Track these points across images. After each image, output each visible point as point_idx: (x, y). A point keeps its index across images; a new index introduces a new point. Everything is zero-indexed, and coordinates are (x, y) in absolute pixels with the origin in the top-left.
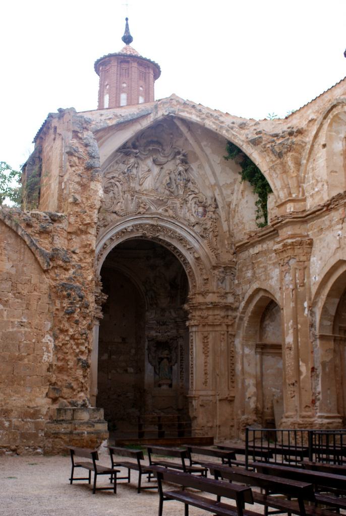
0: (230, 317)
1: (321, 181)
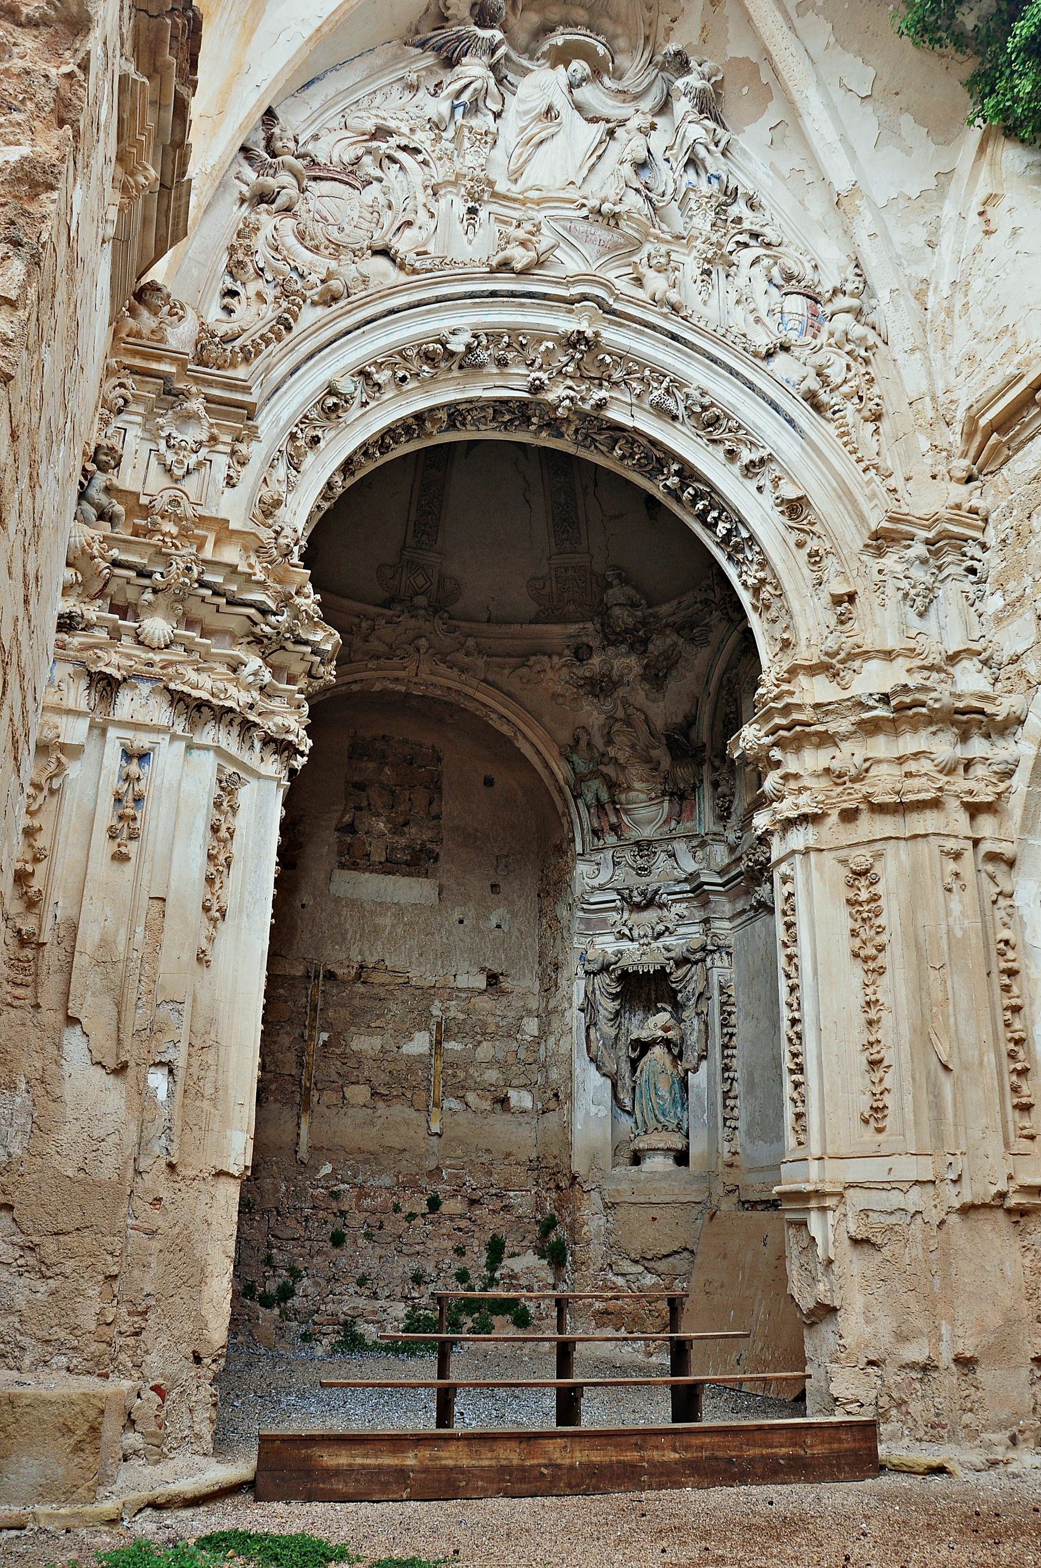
0: (979, 770)
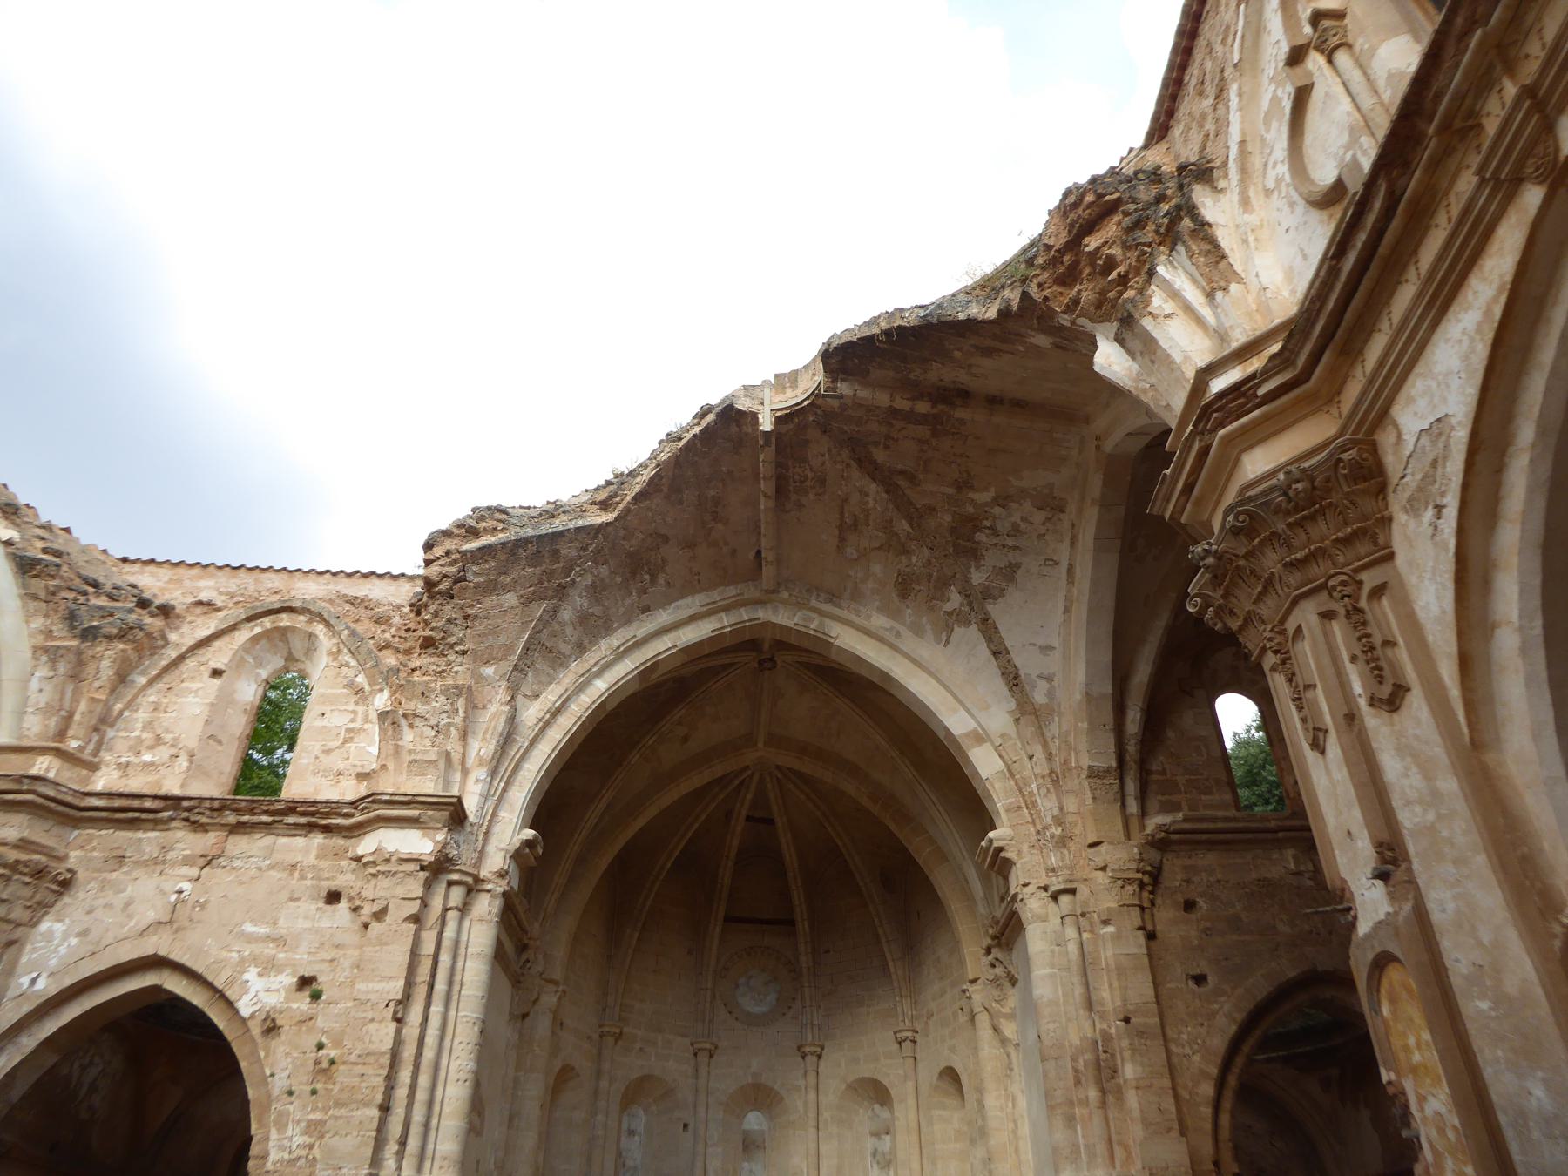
1: (173, 746)
